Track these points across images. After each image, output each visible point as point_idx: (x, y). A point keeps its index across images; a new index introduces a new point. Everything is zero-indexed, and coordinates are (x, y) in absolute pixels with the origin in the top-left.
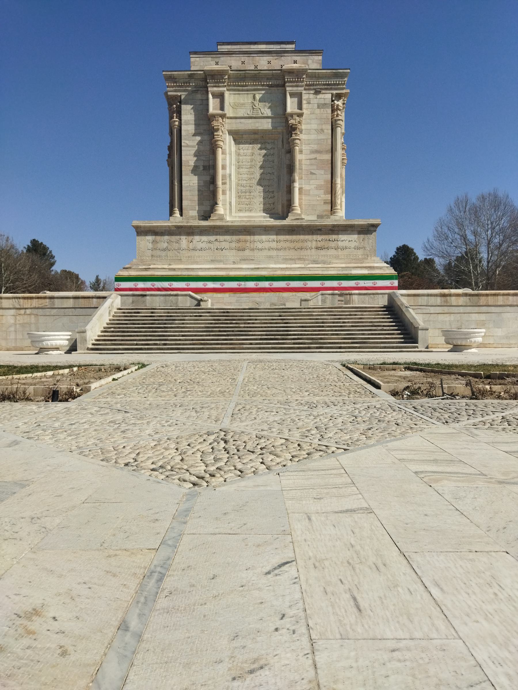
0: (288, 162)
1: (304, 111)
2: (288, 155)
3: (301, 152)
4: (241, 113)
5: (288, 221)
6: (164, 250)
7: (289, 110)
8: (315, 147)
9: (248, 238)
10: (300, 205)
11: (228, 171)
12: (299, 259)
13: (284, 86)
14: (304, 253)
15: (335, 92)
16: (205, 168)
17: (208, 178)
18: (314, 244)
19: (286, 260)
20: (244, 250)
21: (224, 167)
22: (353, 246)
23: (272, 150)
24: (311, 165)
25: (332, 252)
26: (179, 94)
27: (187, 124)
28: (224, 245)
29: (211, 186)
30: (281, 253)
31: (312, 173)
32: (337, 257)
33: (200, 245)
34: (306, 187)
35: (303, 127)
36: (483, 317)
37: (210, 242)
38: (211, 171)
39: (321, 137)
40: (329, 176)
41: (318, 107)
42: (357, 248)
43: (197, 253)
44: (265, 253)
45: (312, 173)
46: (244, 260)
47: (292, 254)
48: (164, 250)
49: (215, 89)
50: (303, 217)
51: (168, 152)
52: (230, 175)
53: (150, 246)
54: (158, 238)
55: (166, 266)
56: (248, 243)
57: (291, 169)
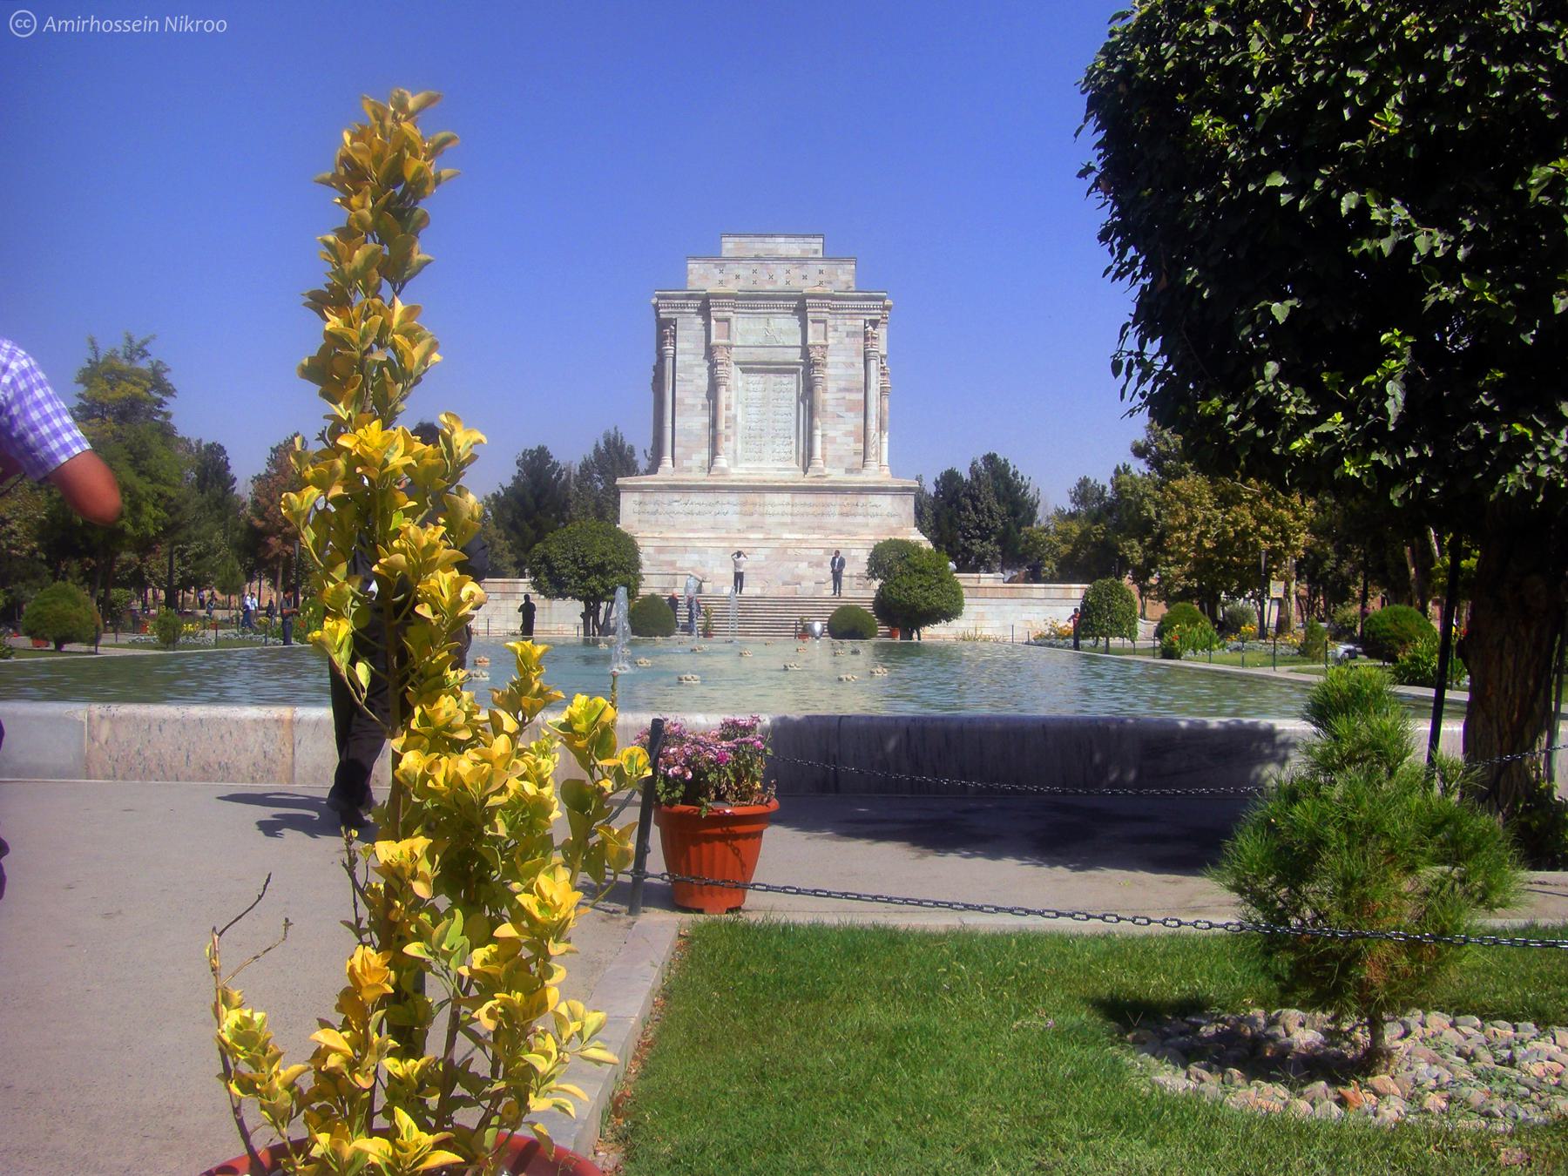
1: (830, 341)
3: (825, 390)
4: (752, 340)
7: (810, 341)
8: (843, 384)
10: (824, 456)
11: (733, 411)
12: (819, 527)
14: (826, 520)
18: (837, 510)
19: (803, 529)
20: (752, 514)
21: (728, 408)
25: (860, 519)
27: (684, 353)
30: (797, 519)
33: (697, 509)
34: (831, 433)
35: (829, 359)
36: (981, 609)
39: (851, 371)
43: (695, 518)
46: (752, 528)
50: (827, 471)
52: (735, 417)
53: (637, 508)
54: (648, 498)
57: (811, 412)
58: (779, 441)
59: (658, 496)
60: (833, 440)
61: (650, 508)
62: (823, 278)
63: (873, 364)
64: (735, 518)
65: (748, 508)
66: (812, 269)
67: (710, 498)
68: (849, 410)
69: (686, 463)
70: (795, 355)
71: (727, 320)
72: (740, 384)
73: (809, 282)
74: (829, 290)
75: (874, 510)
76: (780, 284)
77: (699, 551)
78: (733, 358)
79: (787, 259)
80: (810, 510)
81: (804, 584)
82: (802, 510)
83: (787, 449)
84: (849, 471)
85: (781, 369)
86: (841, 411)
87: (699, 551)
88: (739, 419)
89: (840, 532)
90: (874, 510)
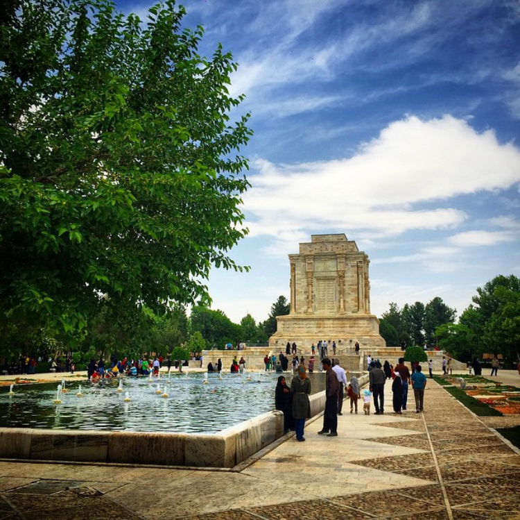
3: (344, 285)
4: (320, 269)
8: (350, 283)
9: (321, 322)
12: (343, 331)
14: (345, 329)
16: (305, 292)
17: (306, 296)
18: (348, 325)
25: (356, 329)
27: (298, 274)
28: (311, 326)
33: (302, 326)
34: (347, 300)
40: (357, 295)
42: (367, 327)
44: (329, 329)
47: (340, 329)
51: (290, 282)
54: (286, 323)
59: (288, 323)
62: (344, 248)
63: (360, 276)
65: (319, 325)
66: (340, 245)
67: (307, 322)
68: (352, 291)
69: (299, 311)
73: (339, 249)
74: (345, 252)
76: (330, 250)
77: (301, 340)
78: (314, 276)
79: (332, 242)
84: (353, 312)
86: (350, 292)
87: (301, 340)
89: (350, 333)
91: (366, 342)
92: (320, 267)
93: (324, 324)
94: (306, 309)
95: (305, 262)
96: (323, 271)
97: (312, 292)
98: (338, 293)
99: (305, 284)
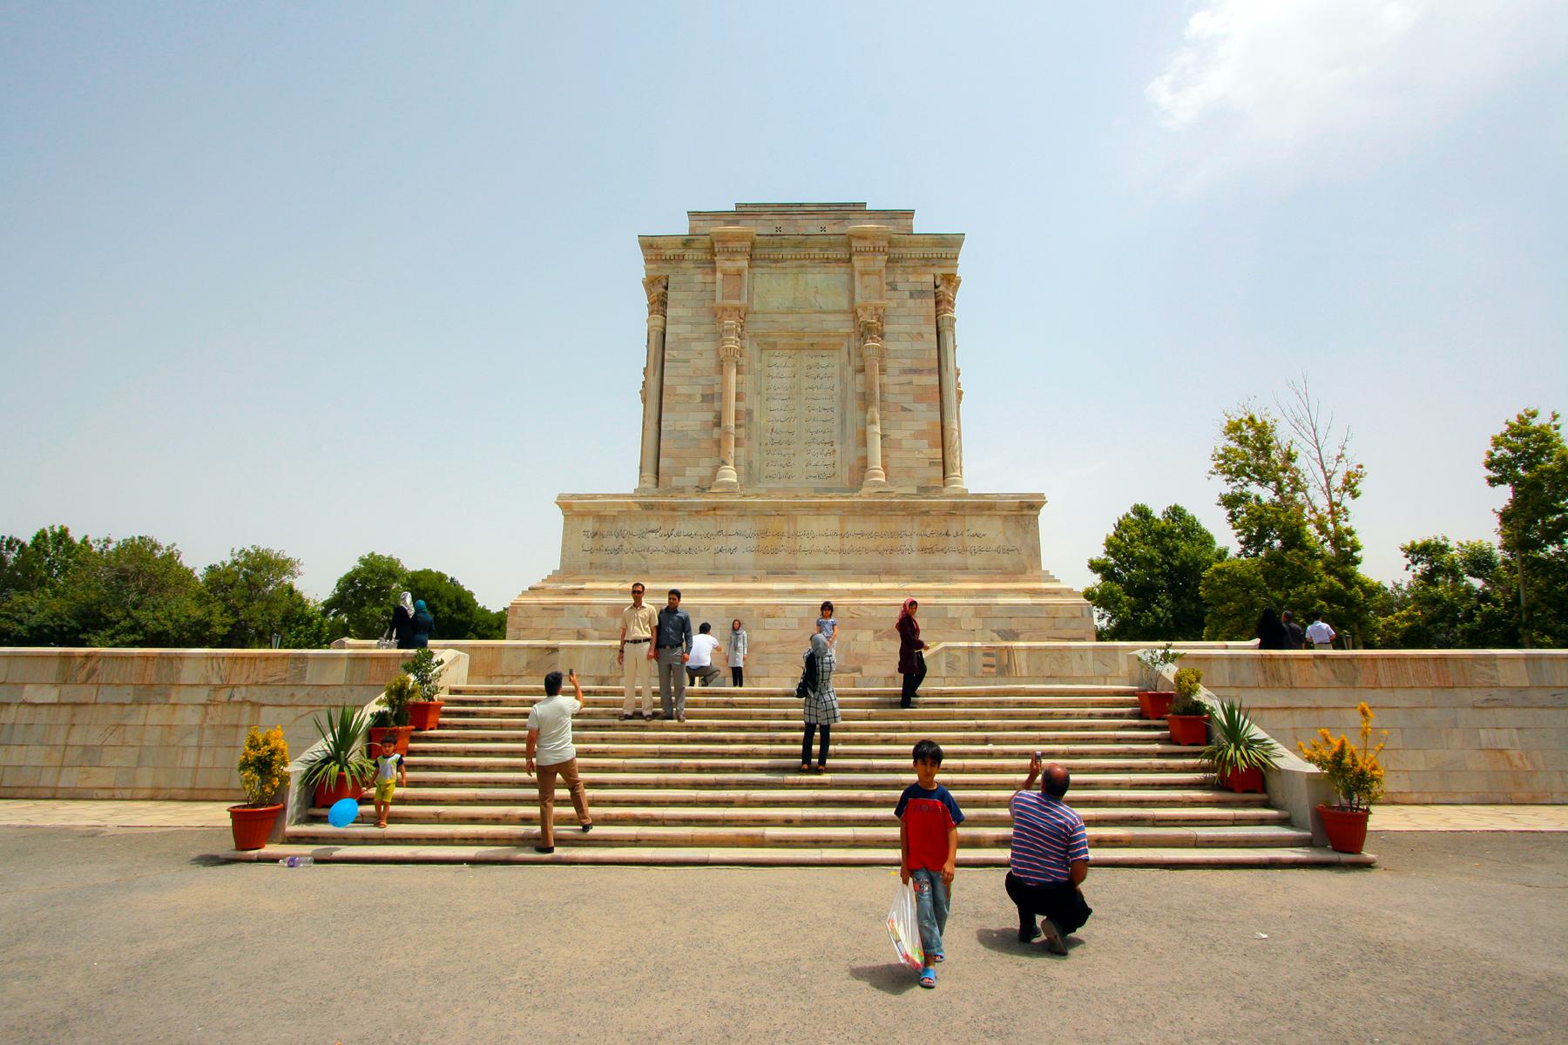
0: (859, 389)
2: (860, 377)
3: (883, 371)
4: (775, 302)
5: (865, 495)
6: (616, 551)
8: (908, 363)
10: (885, 467)
13: (849, 260)
15: (939, 272)
16: (708, 398)
17: (710, 417)
18: (914, 542)
20: (775, 552)
22: (994, 547)
23: (830, 370)
24: (902, 394)
26: (664, 273)
27: (677, 321)
29: (716, 430)
31: (904, 409)
32: (964, 569)
33: (686, 543)
34: (895, 434)
35: (887, 329)
37: (707, 536)
38: (717, 405)
39: (919, 345)
41: (912, 296)
45: (904, 409)
46: (776, 573)
48: (616, 551)
49: (728, 265)
52: (749, 413)
53: (589, 543)
54: (605, 528)
55: (615, 586)
56: (784, 539)
58: (816, 448)
60: (898, 445)
61: (611, 542)
64: (749, 558)
67: (708, 524)
68: (919, 399)
69: (676, 482)
70: (840, 325)
71: (739, 274)
72: (757, 366)
75: (975, 543)
80: (871, 543)
81: (868, 670)
82: (856, 542)
83: (829, 460)
85: (818, 345)
88: (756, 415)
90: (975, 543)
91: (1014, 625)
92: (775, 291)
93: (796, 535)
94: (707, 472)
95: (714, 271)
96: (791, 311)
97: (739, 397)
98: (853, 404)
99: (706, 362)
